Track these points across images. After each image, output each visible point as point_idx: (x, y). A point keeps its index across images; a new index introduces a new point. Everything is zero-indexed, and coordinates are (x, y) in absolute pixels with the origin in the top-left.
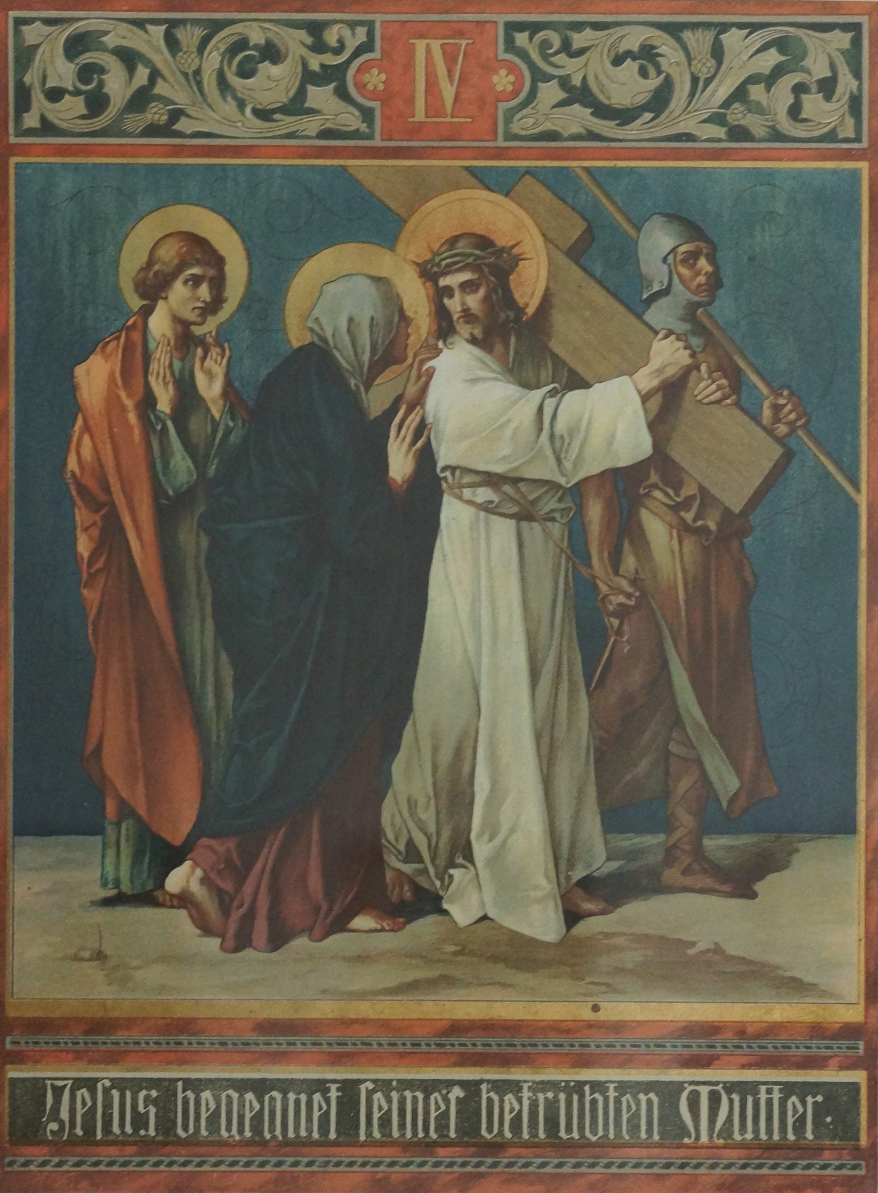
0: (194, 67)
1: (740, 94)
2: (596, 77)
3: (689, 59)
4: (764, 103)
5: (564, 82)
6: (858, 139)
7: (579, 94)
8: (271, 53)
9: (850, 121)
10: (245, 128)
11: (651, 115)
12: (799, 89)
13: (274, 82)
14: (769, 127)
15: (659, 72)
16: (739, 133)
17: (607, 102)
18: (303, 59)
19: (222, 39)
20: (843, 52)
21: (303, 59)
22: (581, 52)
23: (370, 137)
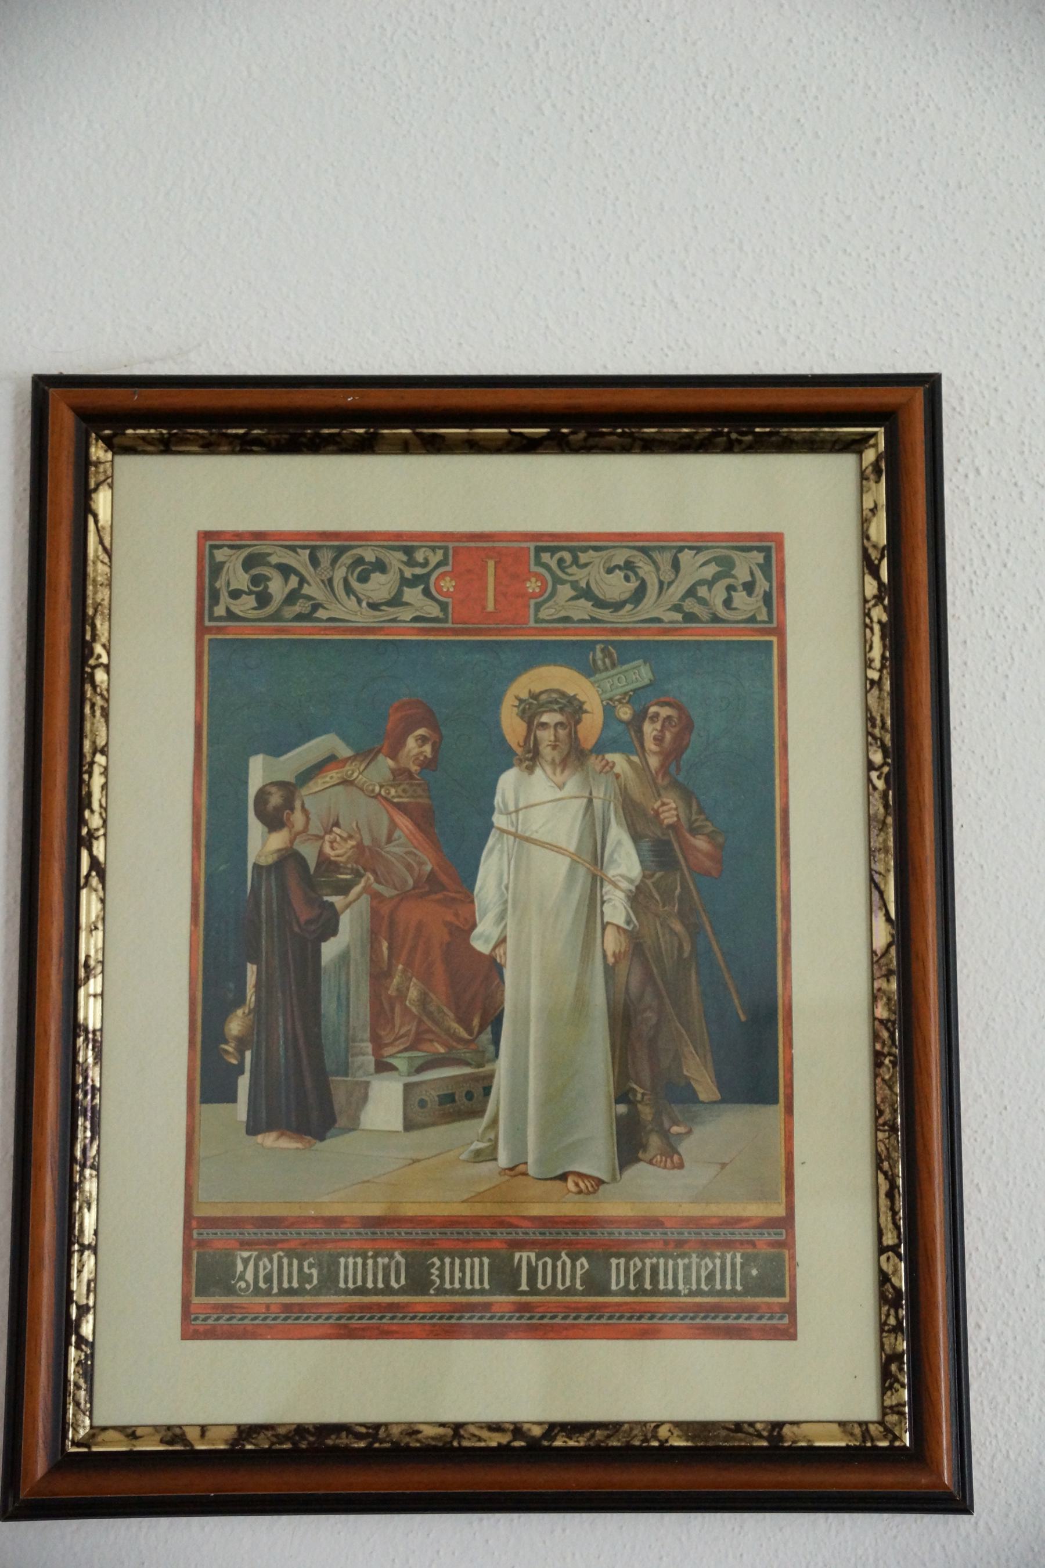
1: (691, 592)
2: (597, 582)
3: (658, 569)
4: (708, 598)
5: (574, 585)
6: (770, 621)
8: (381, 567)
9: (764, 610)
12: (730, 588)
13: (380, 586)
16: (690, 617)
17: (601, 597)
18: (400, 570)
19: (346, 559)
20: (758, 565)
21: (400, 570)
22: (586, 565)
23: (445, 621)
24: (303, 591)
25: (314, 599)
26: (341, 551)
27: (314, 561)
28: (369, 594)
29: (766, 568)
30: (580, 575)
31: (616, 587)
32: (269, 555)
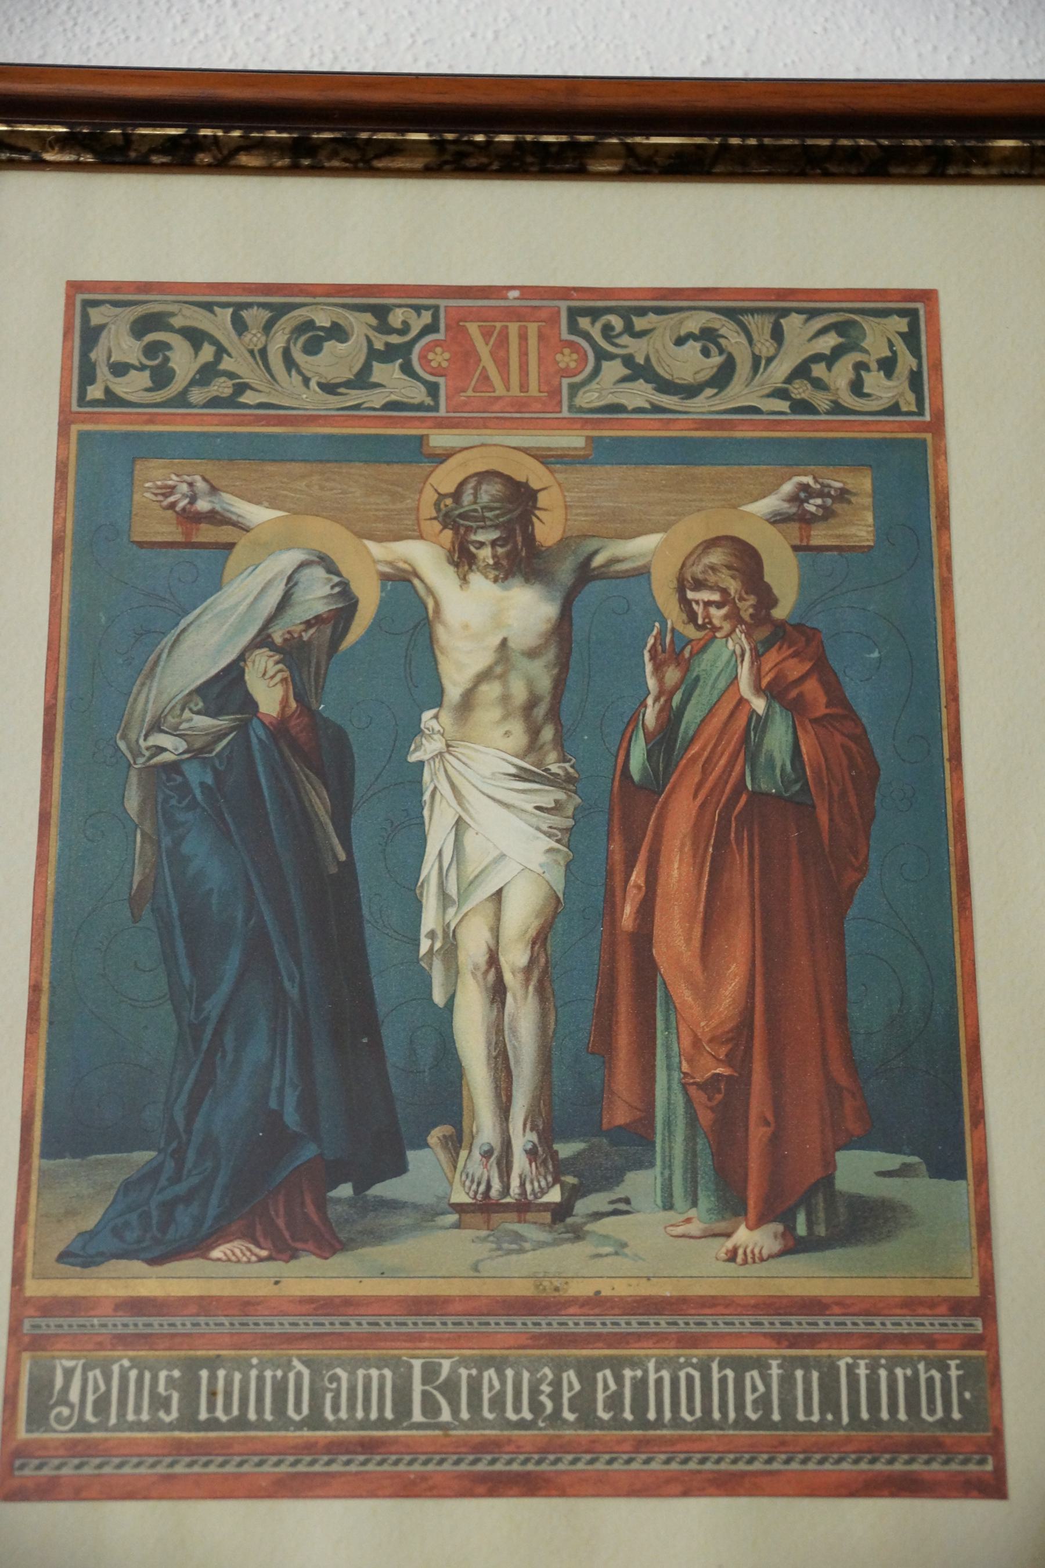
0: (260, 346)
1: (801, 371)
3: (750, 340)
4: (826, 380)
5: (628, 361)
6: (921, 412)
7: (639, 371)
8: (338, 332)
9: (911, 397)
10: (312, 400)
11: (716, 391)
12: (860, 367)
13: (336, 360)
14: (832, 401)
15: (721, 351)
16: (802, 407)
18: (367, 337)
19: (287, 323)
20: (901, 334)
21: (367, 337)
24: (222, 366)
25: (239, 377)
26: (280, 311)
27: (240, 326)
28: (321, 370)
29: (911, 338)
30: (638, 349)
31: (689, 363)
32: (172, 314)
